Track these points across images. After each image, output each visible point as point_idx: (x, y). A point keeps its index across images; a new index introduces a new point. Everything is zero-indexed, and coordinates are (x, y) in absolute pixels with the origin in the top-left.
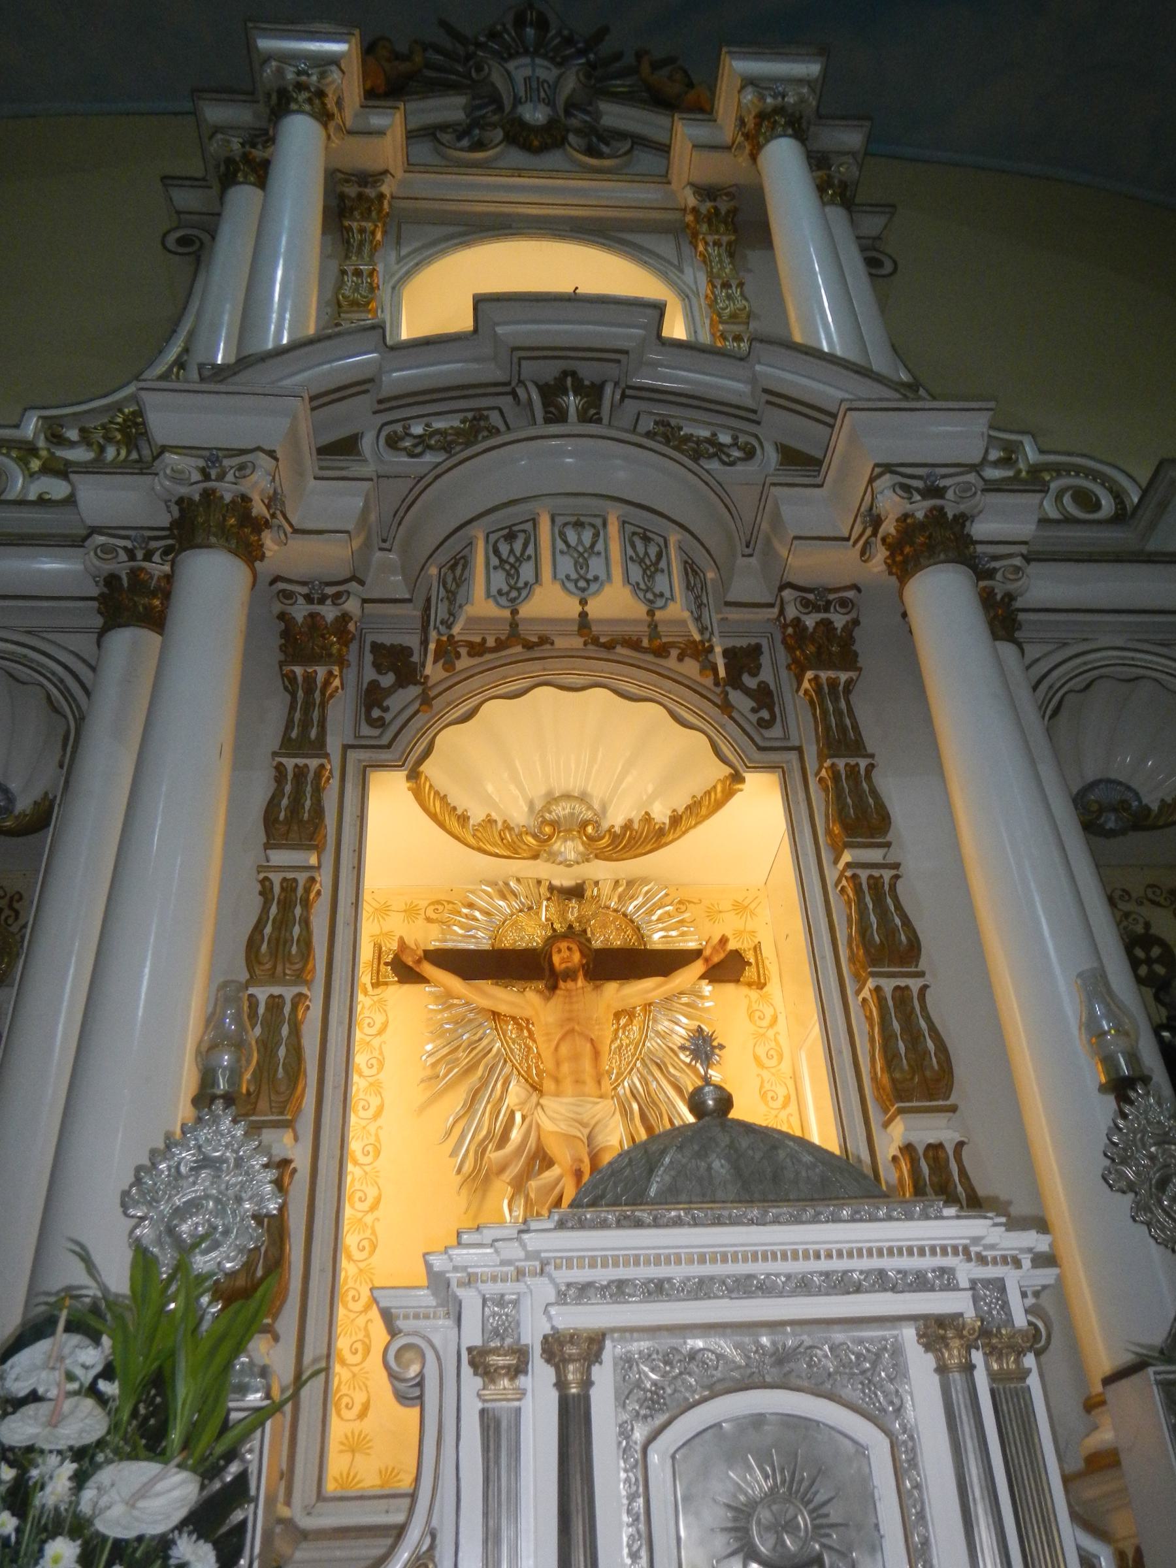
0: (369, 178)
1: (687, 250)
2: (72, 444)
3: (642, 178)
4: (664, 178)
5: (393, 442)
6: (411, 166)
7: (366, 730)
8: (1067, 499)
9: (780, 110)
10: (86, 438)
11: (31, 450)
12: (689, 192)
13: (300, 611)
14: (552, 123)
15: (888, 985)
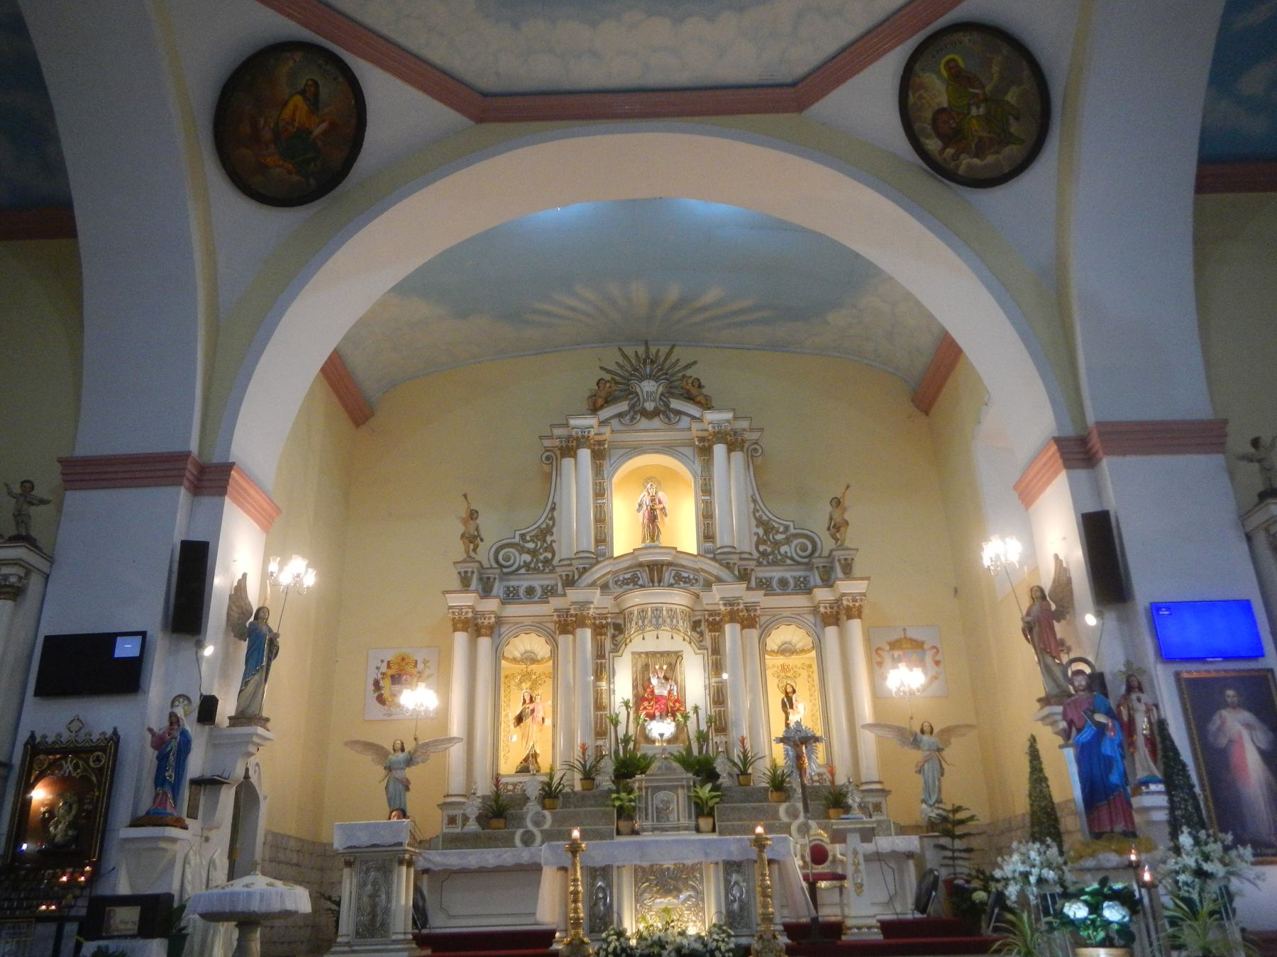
0: (600, 443)
1: (696, 456)
2: (529, 542)
3: (682, 430)
4: (690, 429)
5: (616, 582)
6: (613, 431)
7: (613, 647)
8: (798, 548)
9: (719, 432)
10: (532, 540)
11: (518, 544)
12: (696, 439)
13: (597, 622)
14: (656, 408)
15: (717, 709)
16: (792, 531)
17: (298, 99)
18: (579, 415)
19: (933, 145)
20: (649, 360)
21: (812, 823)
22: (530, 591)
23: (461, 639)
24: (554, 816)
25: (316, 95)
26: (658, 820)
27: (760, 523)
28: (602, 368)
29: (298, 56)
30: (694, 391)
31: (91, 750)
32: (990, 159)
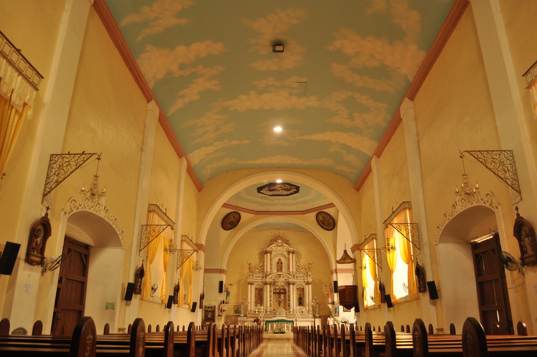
0: (271, 251)
16: (302, 267)
17: (233, 218)
18: (268, 248)
19: (321, 224)
20: (279, 236)
21: (300, 316)
22: (259, 277)
23: (249, 286)
24: (264, 314)
25: (235, 217)
26: (279, 315)
27: (297, 266)
28: (272, 237)
29: (233, 213)
30: (287, 243)
31: (212, 307)
32: (328, 227)
